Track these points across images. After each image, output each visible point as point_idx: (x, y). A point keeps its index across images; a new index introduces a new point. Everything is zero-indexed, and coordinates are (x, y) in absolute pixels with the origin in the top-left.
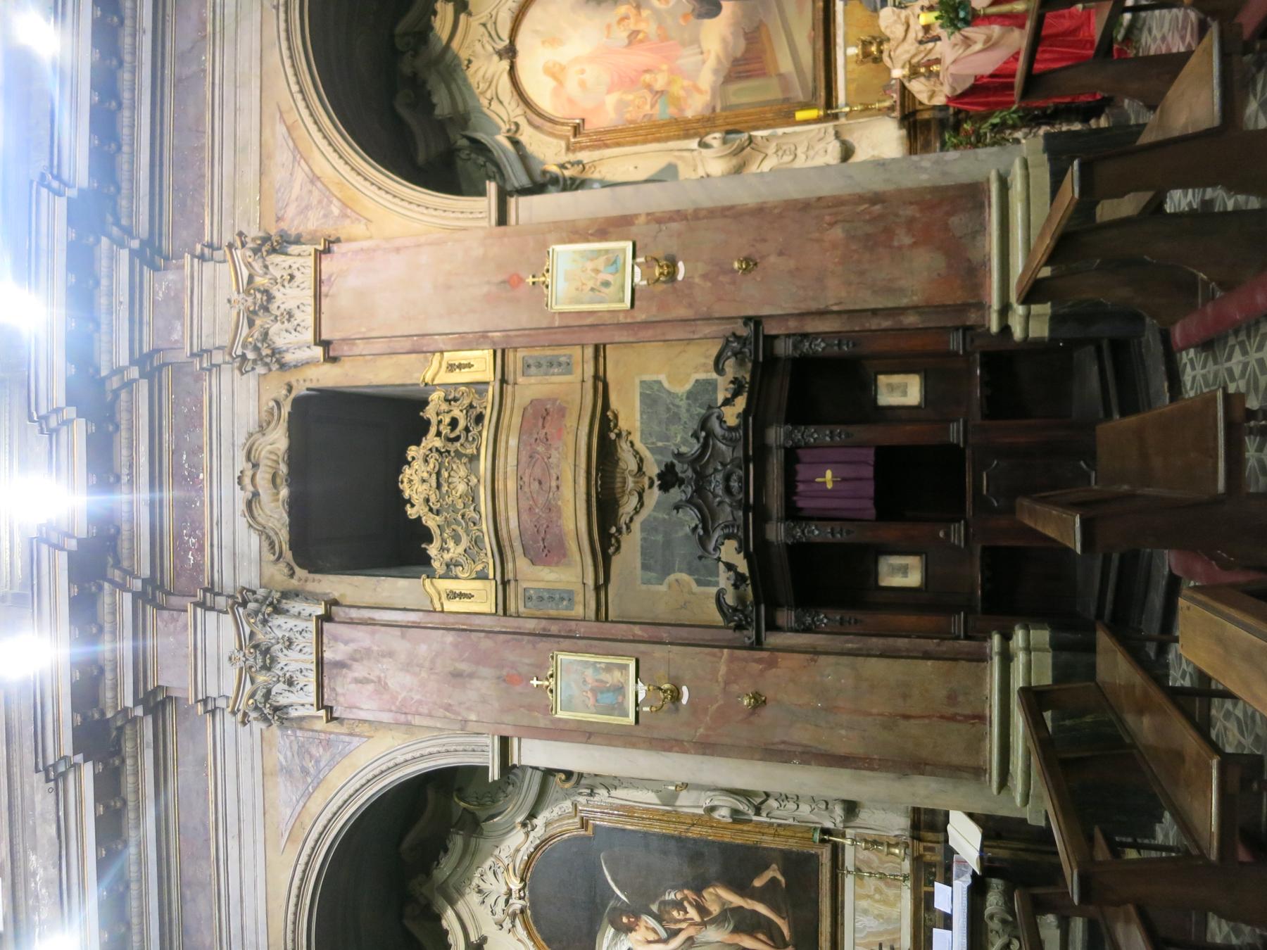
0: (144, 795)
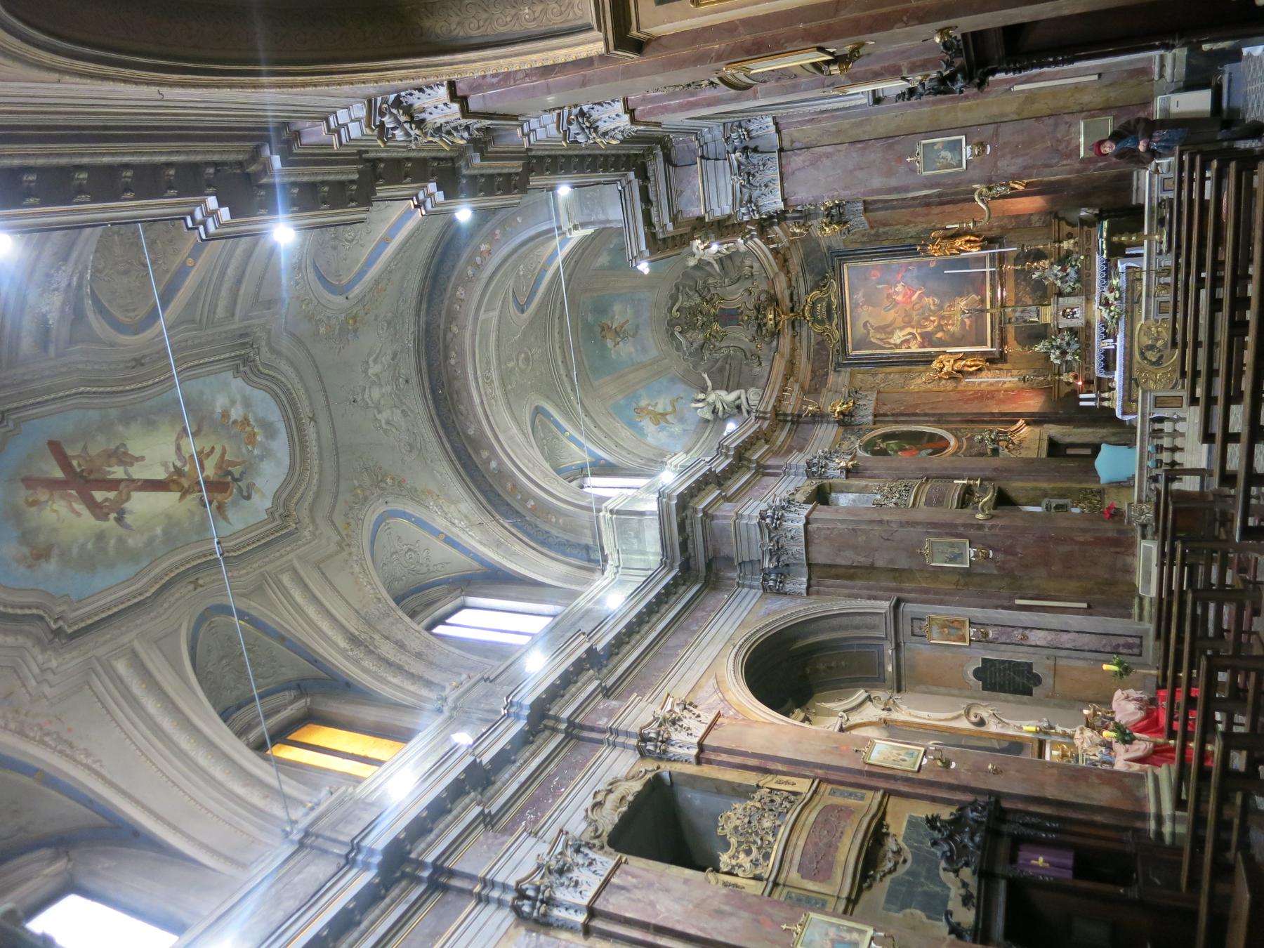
0: (374, 930)
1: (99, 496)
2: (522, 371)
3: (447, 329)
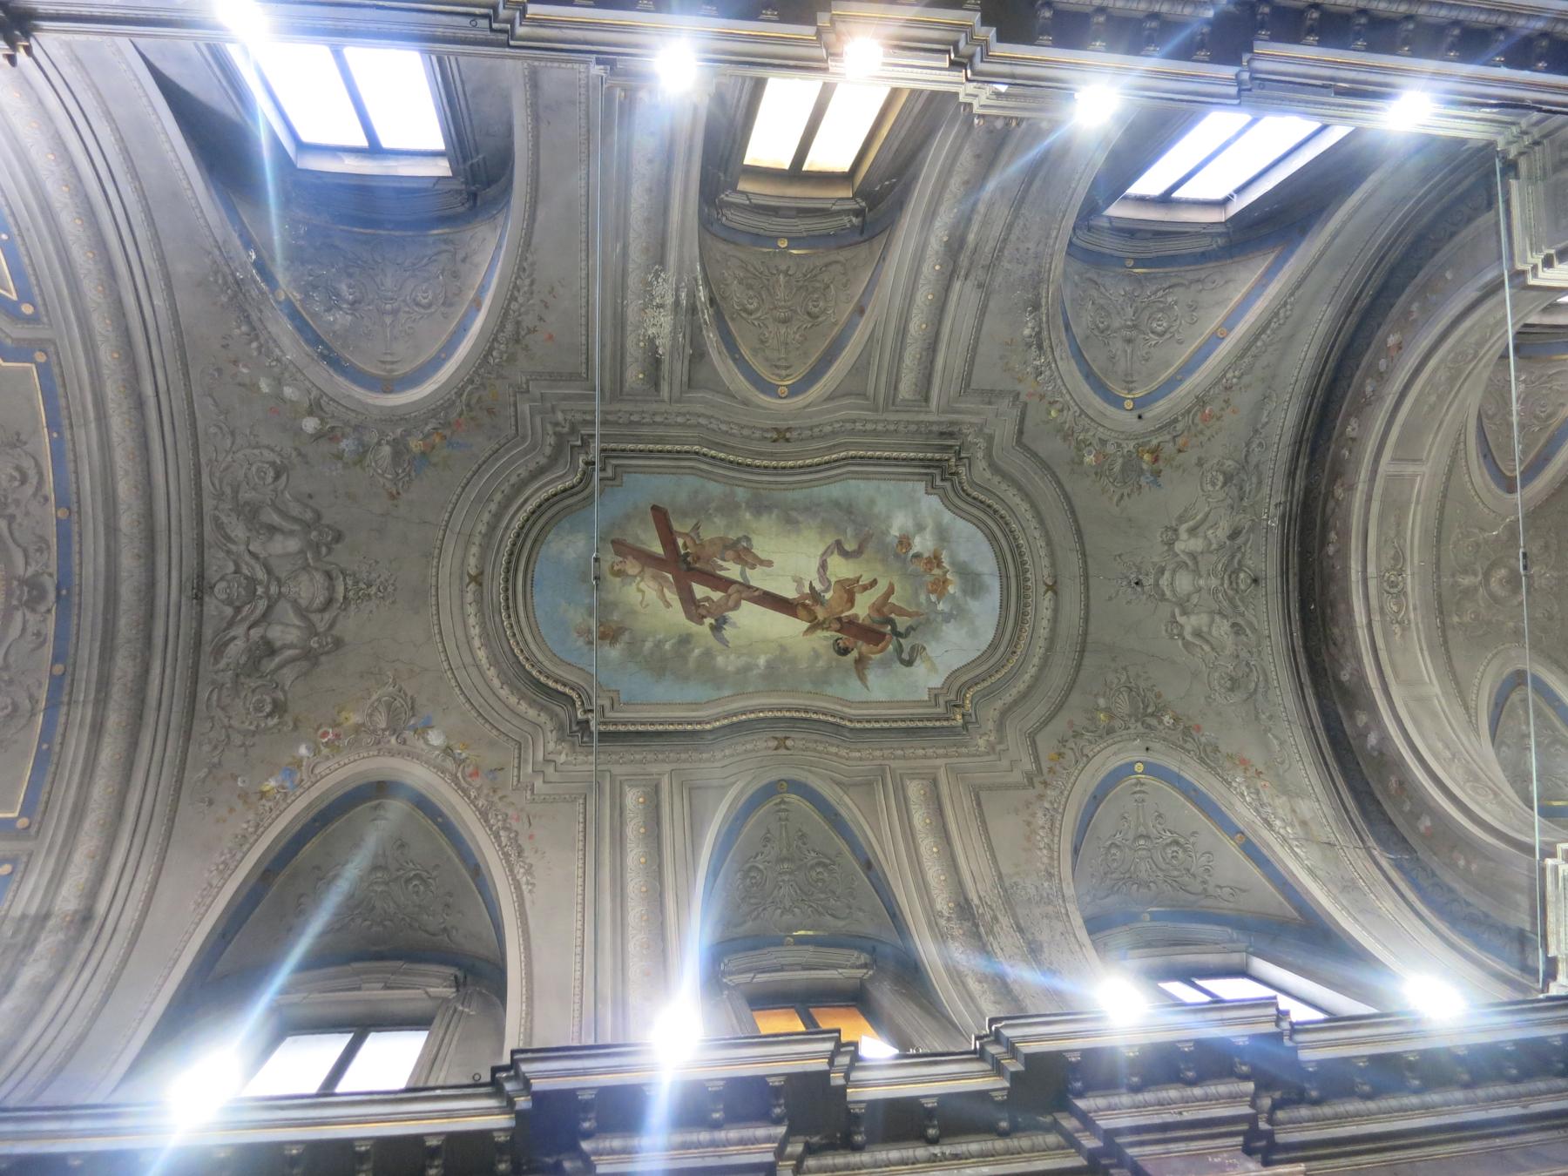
1: (700, 591)
2: (1494, 598)
3: (1330, 493)
